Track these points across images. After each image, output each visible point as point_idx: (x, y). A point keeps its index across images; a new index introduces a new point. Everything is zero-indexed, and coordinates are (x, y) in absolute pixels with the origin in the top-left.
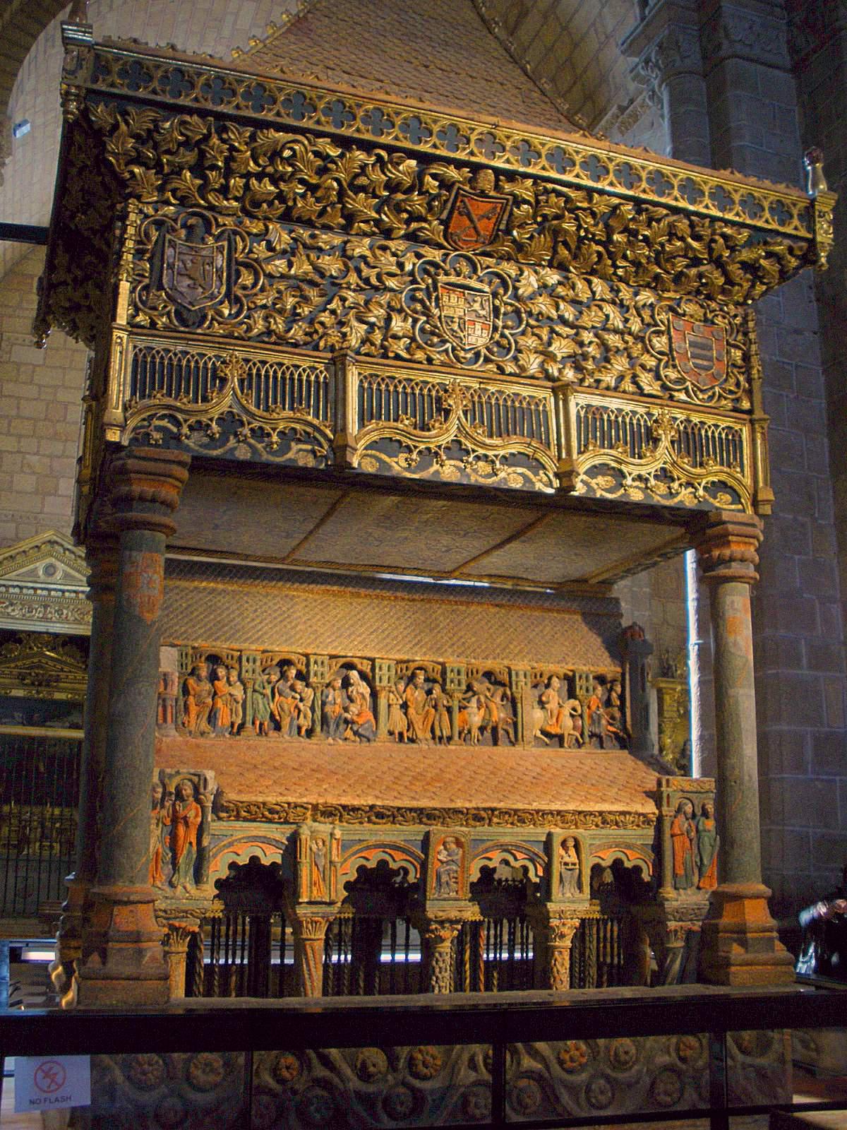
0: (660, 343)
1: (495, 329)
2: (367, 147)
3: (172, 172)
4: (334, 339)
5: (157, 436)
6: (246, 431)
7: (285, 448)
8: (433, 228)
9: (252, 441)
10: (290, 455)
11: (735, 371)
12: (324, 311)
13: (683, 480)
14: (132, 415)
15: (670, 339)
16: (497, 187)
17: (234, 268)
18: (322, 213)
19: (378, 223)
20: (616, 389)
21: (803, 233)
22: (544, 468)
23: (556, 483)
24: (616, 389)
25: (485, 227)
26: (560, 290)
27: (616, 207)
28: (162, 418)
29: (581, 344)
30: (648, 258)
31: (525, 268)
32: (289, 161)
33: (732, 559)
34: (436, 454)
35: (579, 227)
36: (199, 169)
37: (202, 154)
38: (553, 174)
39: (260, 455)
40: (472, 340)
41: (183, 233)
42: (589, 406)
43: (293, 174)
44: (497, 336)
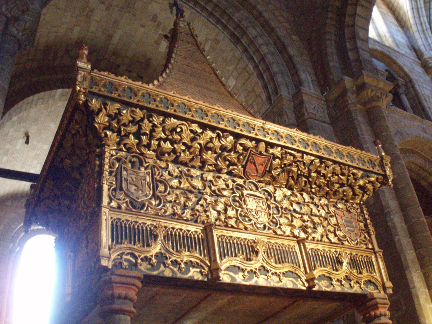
0: (333, 221)
1: (270, 215)
2: (213, 129)
3: (125, 135)
4: (204, 218)
5: (125, 264)
6: (169, 262)
7: (188, 271)
8: (238, 169)
9: (171, 267)
10: (190, 274)
11: (363, 232)
12: (198, 204)
13: (355, 281)
14: (113, 252)
15: (337, 219)
16: (267, 151)
17: (155, 183)
18: (192, 160)
19: (216, 165)
20: (321, 241)
21: (381, 172)
22: (300, 277)
23: (307, 285)
24: (321, 241)
25: (261, 169)
26: (292, 198)
27: (313, 161)
28: (128, 254)
29: (304, 221)
30: (324, 183)
31: (277, 188)
32: (180, 134)
33: (381, 315)
34: (255, 273)
35: (298, 169)
36: (138, 135)
37: (140, 128)
38: (289, 145)
39: (176, 274)
40: (261, 219)
41: (130, 165)
42: (312, 249)
43: (181, 140)
44: (271, 218)
